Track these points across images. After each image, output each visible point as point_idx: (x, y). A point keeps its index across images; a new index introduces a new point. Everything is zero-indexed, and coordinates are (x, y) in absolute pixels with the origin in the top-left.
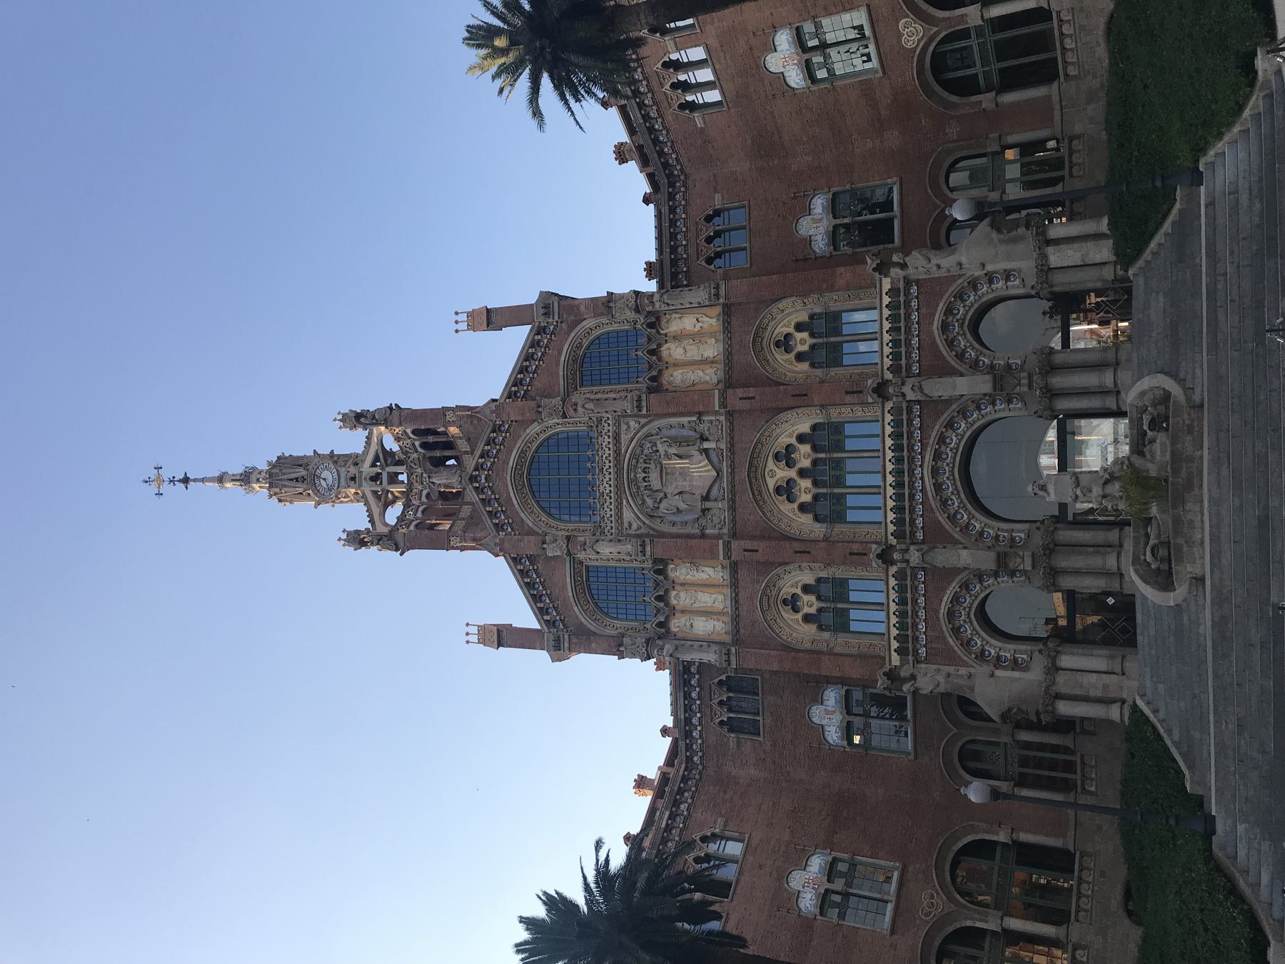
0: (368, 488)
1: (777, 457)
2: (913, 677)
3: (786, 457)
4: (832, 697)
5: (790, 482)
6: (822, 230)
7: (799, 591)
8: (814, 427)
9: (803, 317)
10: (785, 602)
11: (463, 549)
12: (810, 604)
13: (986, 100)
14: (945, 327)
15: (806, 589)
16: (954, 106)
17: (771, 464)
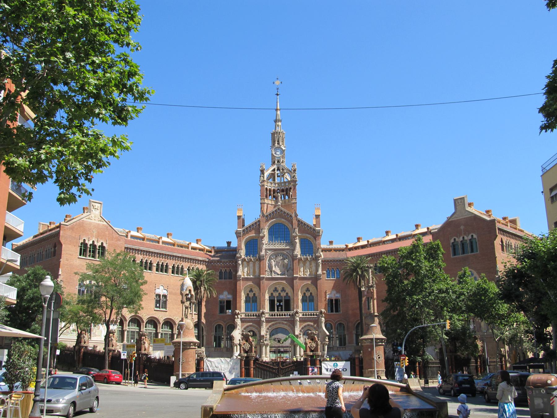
0: (275, 167)
1: (283, 288)
2: (238, 318)
3: (283, 290)
4: (230, 297)
5: (277, 291)
6: (333, 296)
7: (254, 292)
8: (289, 297)
9: (313, 294)
10: (251, 289)
11: (261, 203)
12: (251, 295)
13: (354, 332)
14: (308, 325)
15: (254, 294)
16: (354, 325)
17: (282, 287)
